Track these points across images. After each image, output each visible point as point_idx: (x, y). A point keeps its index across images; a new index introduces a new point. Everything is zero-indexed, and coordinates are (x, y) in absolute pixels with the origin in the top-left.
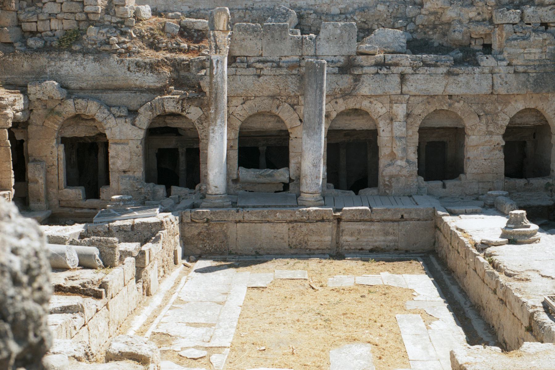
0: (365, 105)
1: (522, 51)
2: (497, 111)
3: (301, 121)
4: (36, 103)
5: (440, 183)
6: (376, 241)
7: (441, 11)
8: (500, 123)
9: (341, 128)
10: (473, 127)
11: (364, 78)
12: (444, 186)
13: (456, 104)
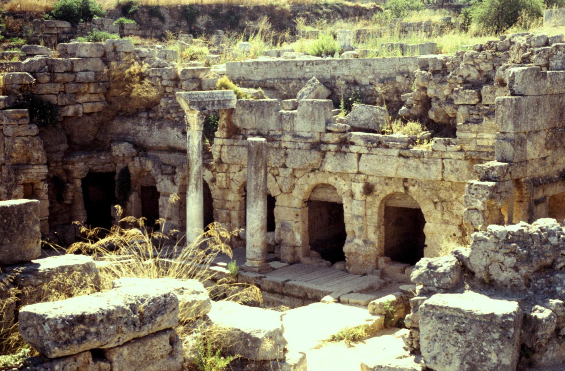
0: (331, 180)
1: (474, 135)
2: (451, 199)
9: (324, 200)
10: (428, 213)
11: (328, 155)
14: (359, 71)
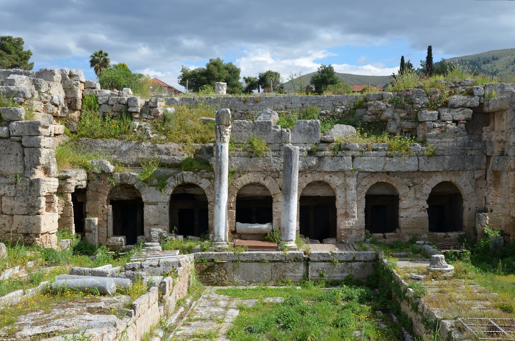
0: (327, 178)
1: (440, 140)
3: (280, 189)
4: (92, 175)
5: (382, 235)
6: (335, 277)
7: (380, 112)
8: (425, 191)
10: (405, 194)
12: (385, 237)
13: (392, 178)
14: (300, 105)
